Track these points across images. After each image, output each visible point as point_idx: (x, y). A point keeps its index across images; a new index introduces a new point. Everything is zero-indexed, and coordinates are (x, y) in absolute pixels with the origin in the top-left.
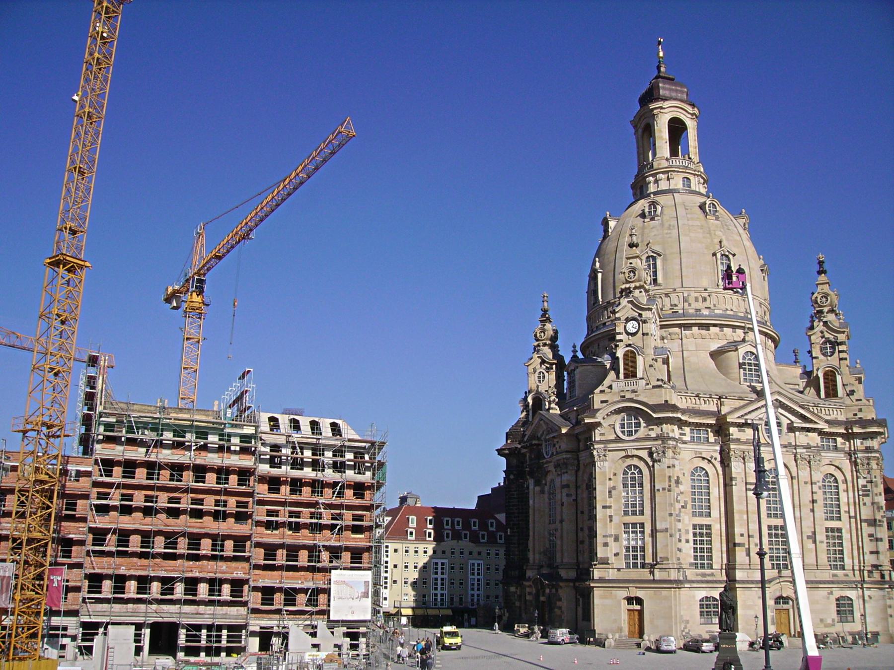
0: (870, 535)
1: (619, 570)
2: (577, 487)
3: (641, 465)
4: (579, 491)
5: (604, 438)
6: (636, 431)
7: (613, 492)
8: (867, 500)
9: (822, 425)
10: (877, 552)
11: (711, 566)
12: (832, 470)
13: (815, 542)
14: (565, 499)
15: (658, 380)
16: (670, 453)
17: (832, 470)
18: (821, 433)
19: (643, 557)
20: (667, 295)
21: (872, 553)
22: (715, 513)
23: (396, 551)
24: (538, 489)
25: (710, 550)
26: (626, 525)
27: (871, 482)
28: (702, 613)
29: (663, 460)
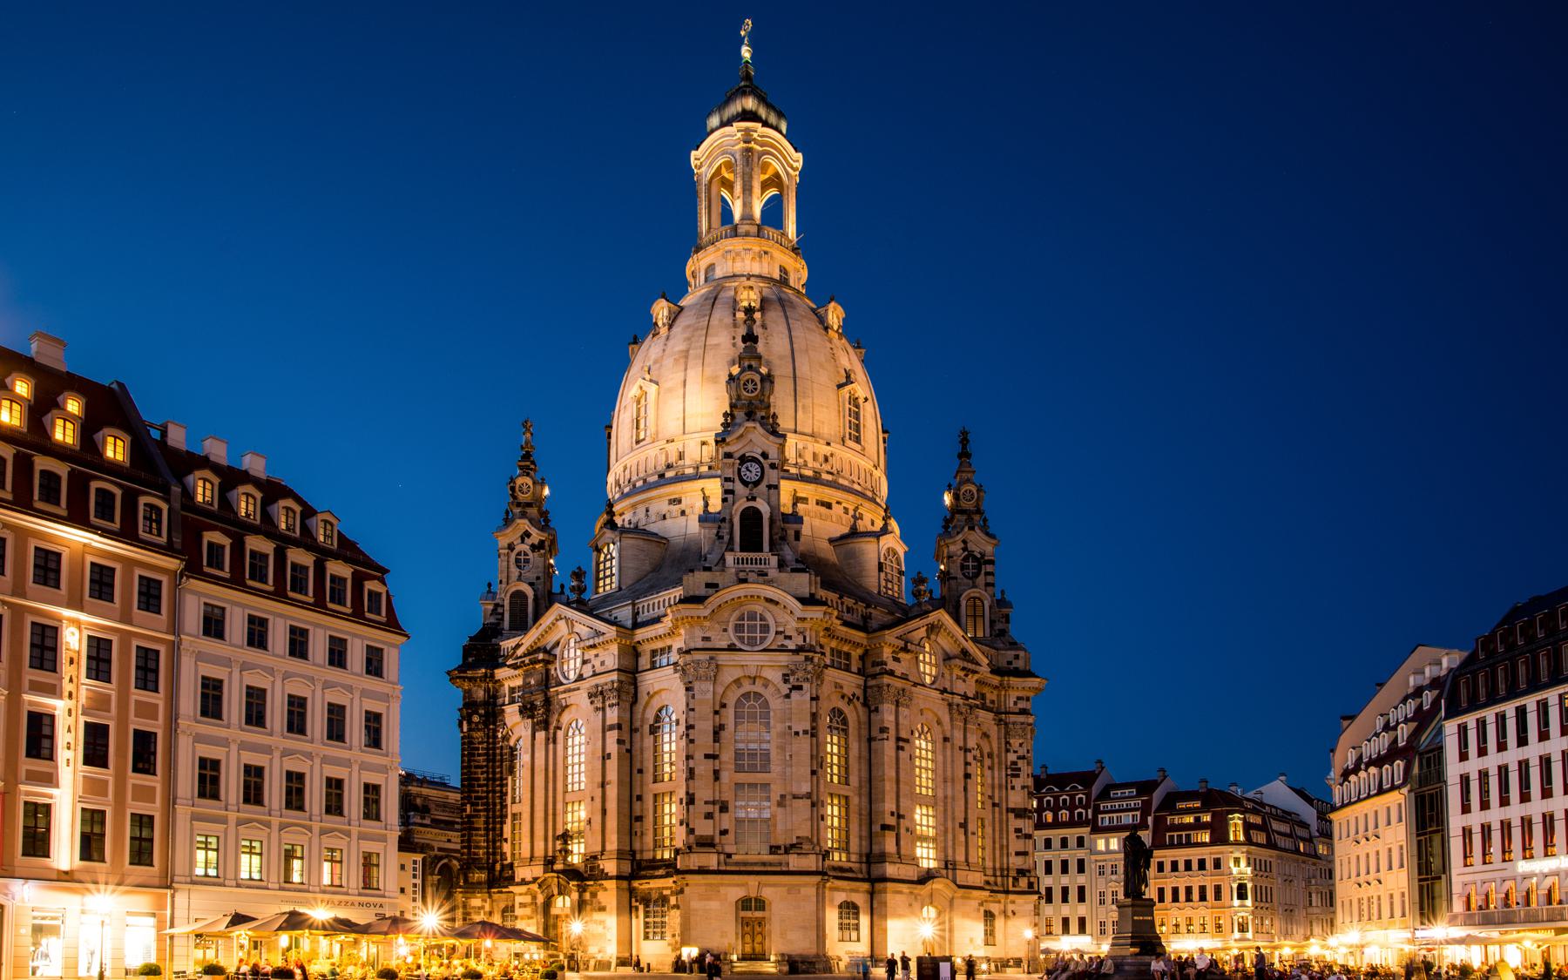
0: (1018, 830)
1: (729, 856)
2: (633, 730)
3: (768, 693)
4: (637, 736)
5: (708, 645)
6: (763, 639)
7: (723, 734)
8: (1018, 783)
10: (1025, 854)
14: (612, 747)
21: (1017, 854)
22: (854, 780)
24: (541, 735)
26: (739, 786)
27: (1023, 758)
29: (806, 686)
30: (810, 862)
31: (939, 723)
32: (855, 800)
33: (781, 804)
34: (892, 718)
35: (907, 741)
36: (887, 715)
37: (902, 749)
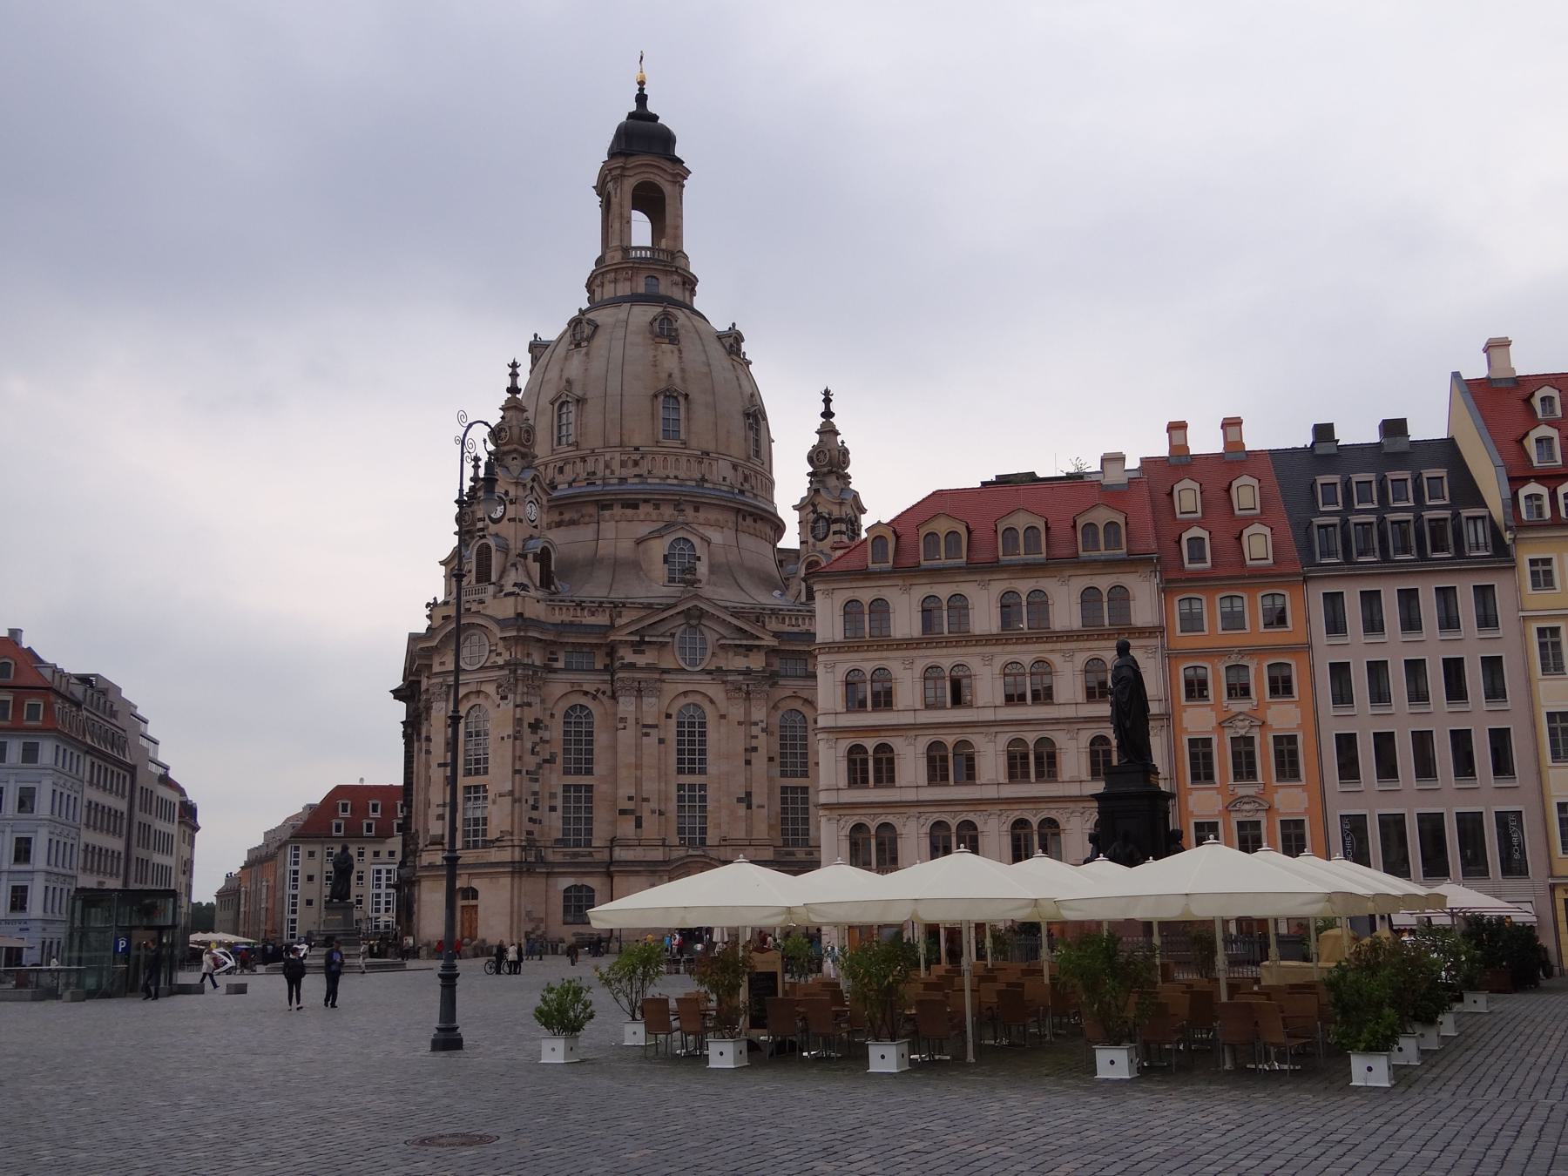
5: (444, 669)
9: (769, 641)
11: (589, 844)
12: (798, 705)
13: (749, 807)
15: (515, 585)
16: (521, 688)
17: (798, 705)
18: (772, 652)
19: (485, 832)
20: (583, 460)
22: (600, 768)
23: (311, 854)
25: (589, 821)
28: (566, 909)
29: (510, 696)
30: (505, 855)
31: (712, 701)
32: (601, 789)
33: (494, 802)
34: (633, 708)
35: (655, 726)
36: (626, 706)
37: (647, 735)
